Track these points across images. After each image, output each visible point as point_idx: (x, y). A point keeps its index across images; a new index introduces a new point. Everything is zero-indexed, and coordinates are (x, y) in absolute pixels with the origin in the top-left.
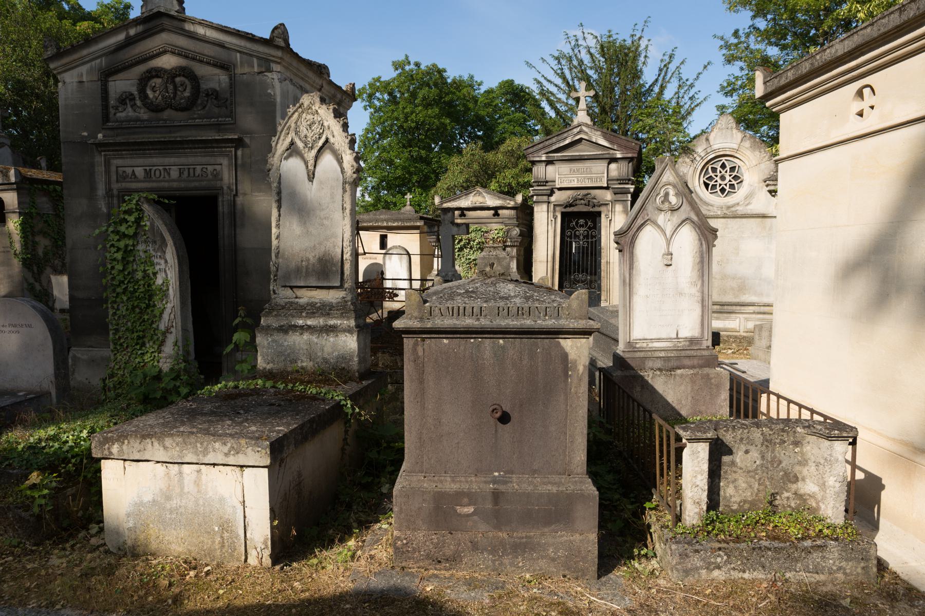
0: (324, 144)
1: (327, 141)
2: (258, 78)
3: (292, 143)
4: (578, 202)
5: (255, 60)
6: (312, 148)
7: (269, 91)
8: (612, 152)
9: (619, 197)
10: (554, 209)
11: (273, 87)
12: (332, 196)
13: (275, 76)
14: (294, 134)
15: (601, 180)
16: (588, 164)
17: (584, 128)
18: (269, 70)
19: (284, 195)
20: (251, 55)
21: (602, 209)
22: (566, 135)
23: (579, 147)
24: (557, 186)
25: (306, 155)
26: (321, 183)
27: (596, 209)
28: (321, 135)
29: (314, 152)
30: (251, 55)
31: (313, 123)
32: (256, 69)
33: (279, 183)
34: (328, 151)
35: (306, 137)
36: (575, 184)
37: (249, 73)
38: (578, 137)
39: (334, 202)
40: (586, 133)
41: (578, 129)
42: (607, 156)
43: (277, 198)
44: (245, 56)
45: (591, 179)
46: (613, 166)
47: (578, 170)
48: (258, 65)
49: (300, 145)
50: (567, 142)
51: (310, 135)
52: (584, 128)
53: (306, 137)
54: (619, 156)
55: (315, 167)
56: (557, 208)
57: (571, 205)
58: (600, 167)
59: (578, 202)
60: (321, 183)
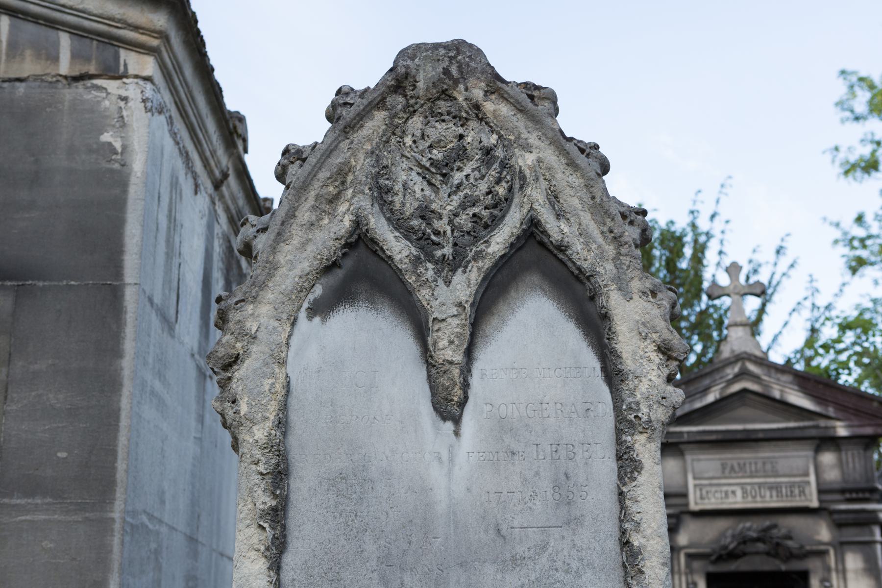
0: (516, 246)
1: (533, 230)
2: (68, 94)
3: (360, 240)
4: (750, 548)
5: (65, 40)
6: (455, 263)
7: (106, 137)
8: (822, 423)
9: (851, 534)
10: (688, 566)
11: (123, 124)
12: (565, 492)
13: (132, 90)
14: (364, 203)
15: (802, 492)
16: (765, 453)
17: (751, 367)
18: (115, 73)
19: (303, 485)
20: (52, 24)
21: (813, 565)
22: (706, 382)
23: (743, 411)
24: (693, 507)
25: (424, 294)
26: (502, 427)
27: (796, 566)
28: (500, 206)
29: (464, 285)
30: (52, 24)
31: (461, 154)
32: (65, 67)
33: (282, 424)
34: (535, 278)
35: (425, 213)
36: (737, 501)
37: (37, 78)
38: (736, 387)
39: (573, 522)
40: (756, 378)
41: (737, 369)
42: (813, 433)
43: (266, 501)
44: (30, 28)
45: (775, 487)
46: (828, 458)
47: (742, 467)
48: (75, 56)
49: (398, 248)
50: (711, 398)
51: (445, 204)
52: (751, 367)
53: (425, 213)
54: (842, 431)
55: (469, 354)
56: (697, 564)
57: (732, 556)
58: (795, 460)
59: (750, 548)
60: (502, 427)
